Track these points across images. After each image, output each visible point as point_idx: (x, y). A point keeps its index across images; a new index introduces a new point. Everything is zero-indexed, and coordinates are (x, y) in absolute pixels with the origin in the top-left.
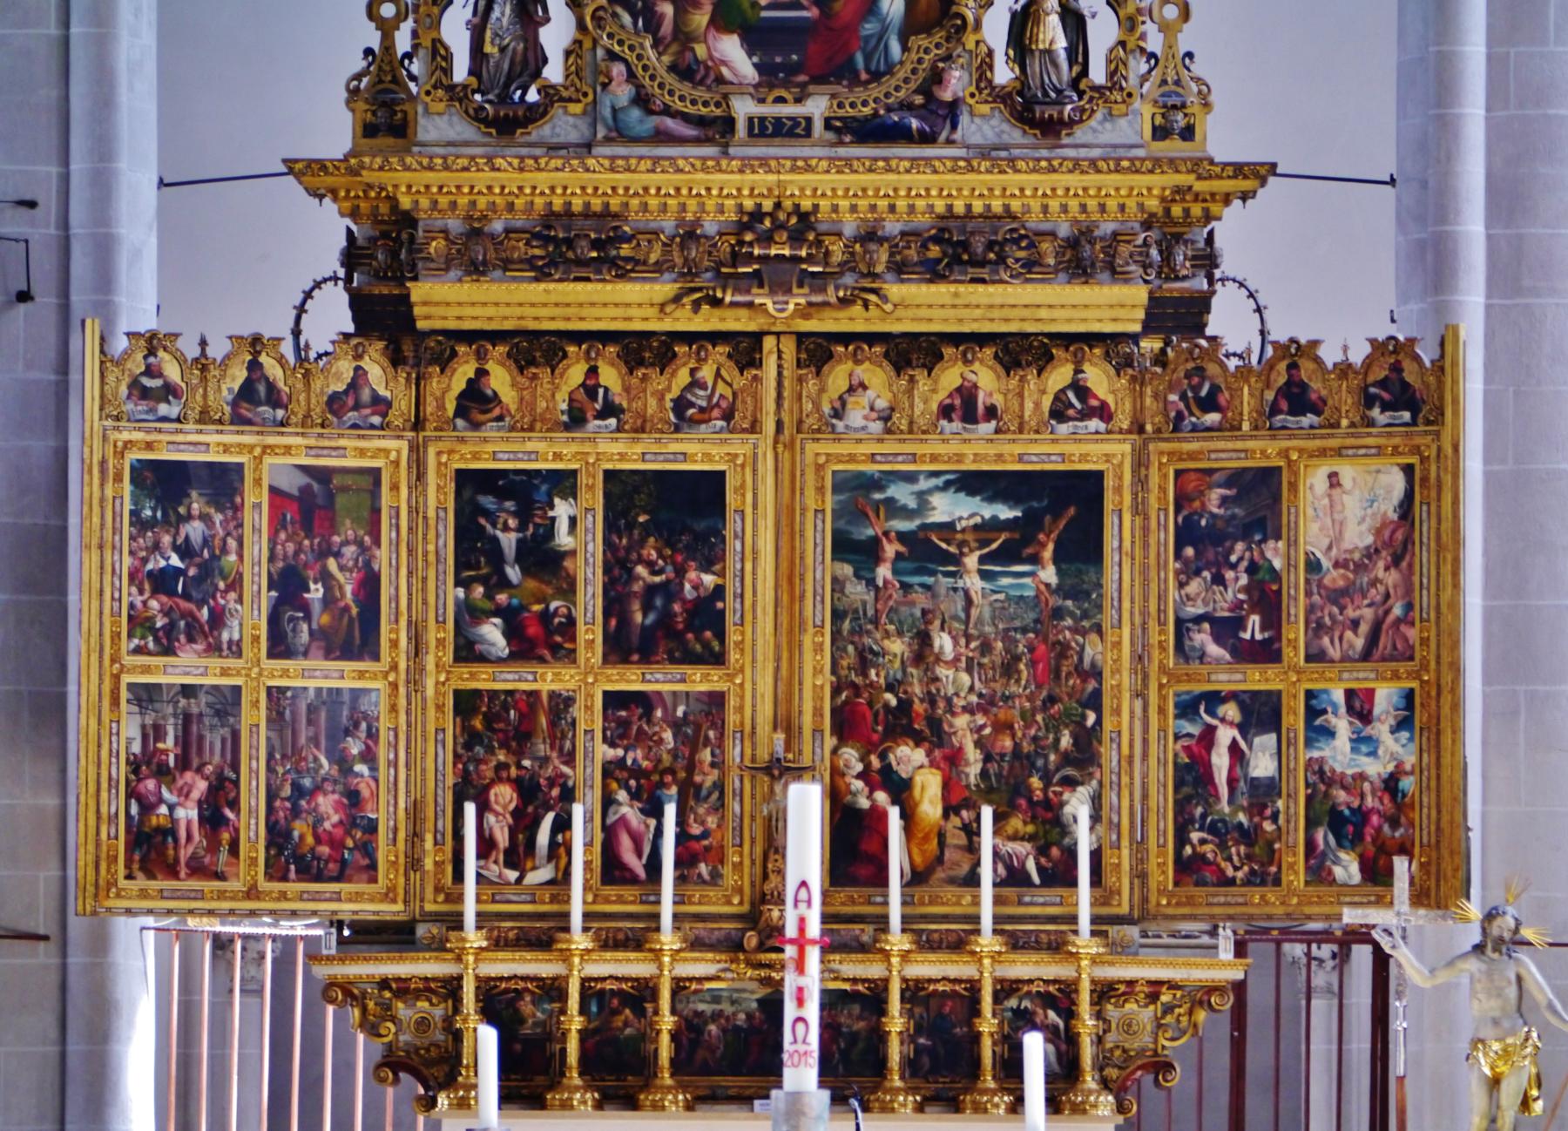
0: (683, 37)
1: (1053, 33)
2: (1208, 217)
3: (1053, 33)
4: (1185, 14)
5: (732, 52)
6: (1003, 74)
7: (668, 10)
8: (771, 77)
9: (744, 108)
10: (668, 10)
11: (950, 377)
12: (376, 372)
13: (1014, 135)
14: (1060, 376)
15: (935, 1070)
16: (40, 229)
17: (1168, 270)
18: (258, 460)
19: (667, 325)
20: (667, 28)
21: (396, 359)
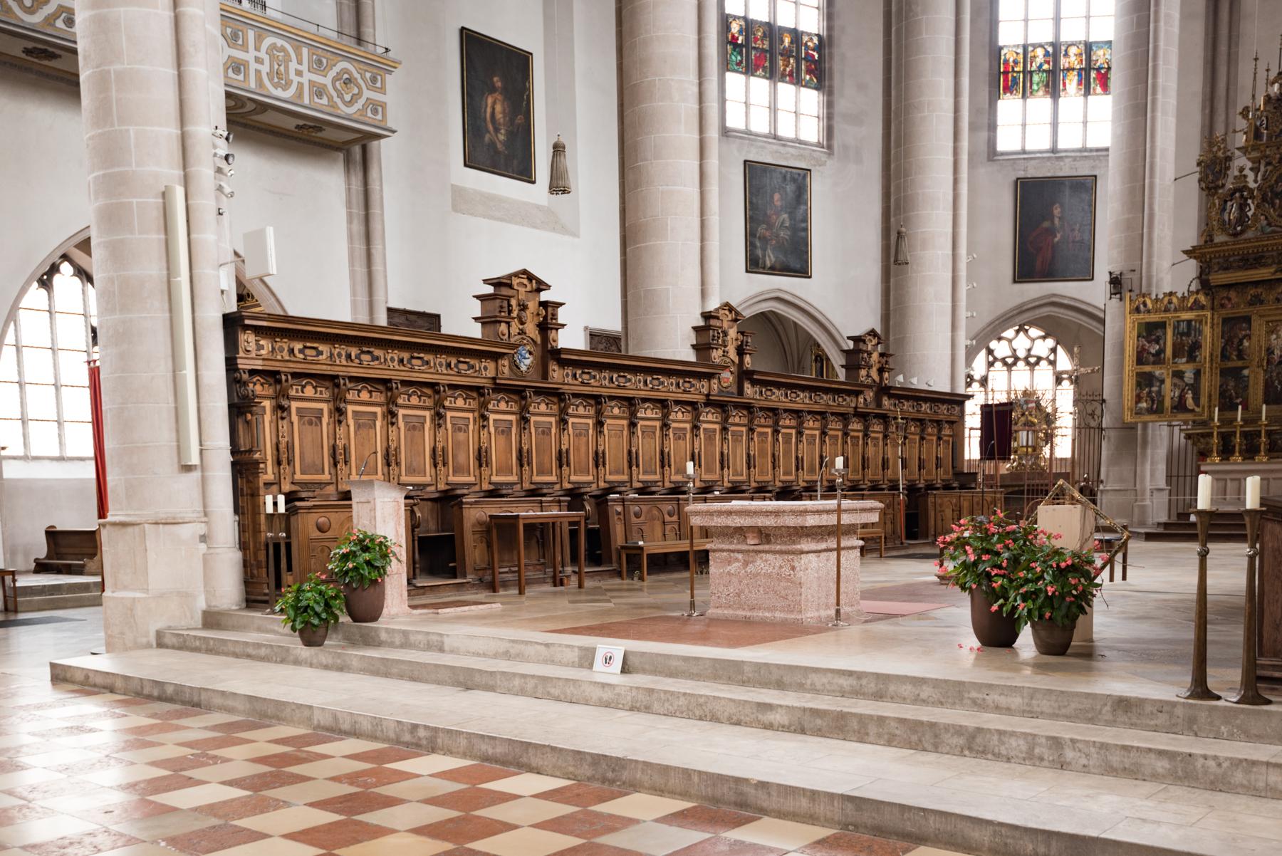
12: (1202, 298)
16: (1135, 276)
18: (1170, 320)
19: (1273, 277)
21: (1206, 295)
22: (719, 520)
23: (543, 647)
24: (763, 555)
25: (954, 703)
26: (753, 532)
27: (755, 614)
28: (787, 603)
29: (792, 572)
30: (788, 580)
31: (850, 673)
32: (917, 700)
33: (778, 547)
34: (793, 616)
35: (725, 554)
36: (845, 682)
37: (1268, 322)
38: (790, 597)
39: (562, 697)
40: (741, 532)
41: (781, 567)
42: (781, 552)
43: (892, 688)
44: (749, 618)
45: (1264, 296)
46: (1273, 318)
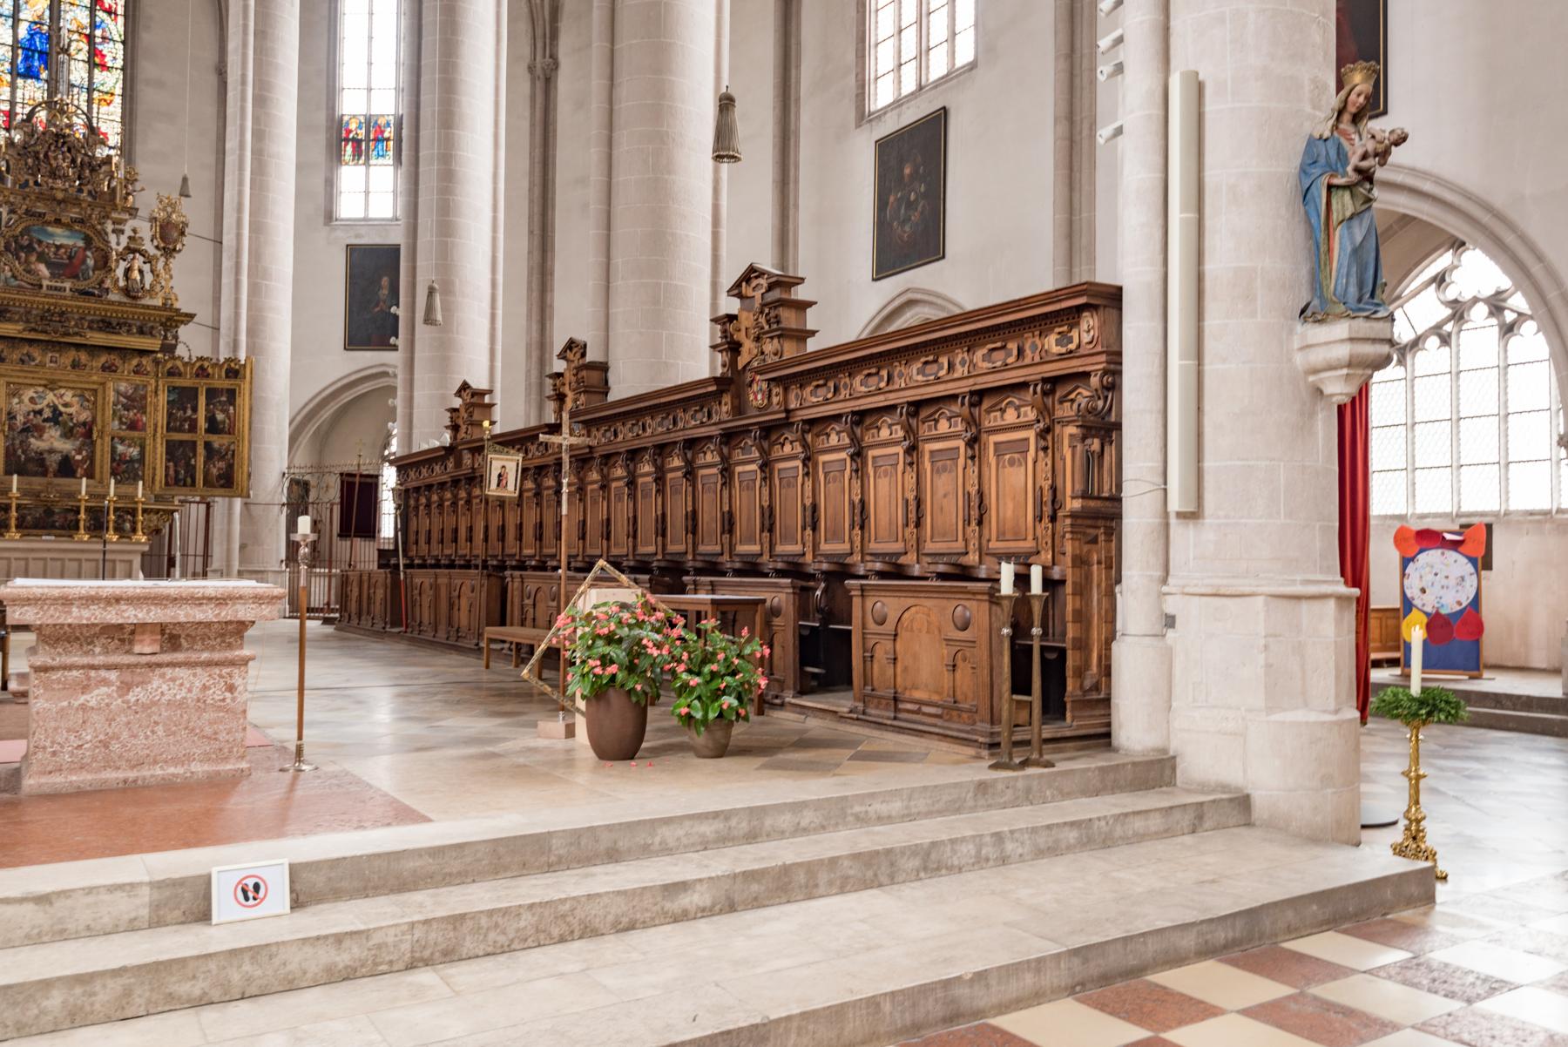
0: (27, 261)
1: (136, 275)
2: (177, 327)
3: (136, 275)
4: (171, 277)
5: (43, 269)
6: (122, 283)
7: (23, 255)
8: (53, 276)
9: (45, 283)
10: (23, 255)
11: (103, 359)
13: (125, 300)
14: (135, 362)
15: (95, 530)
17: (165, 337)
20: (23, 260)
22: (86, 613)
23: (30, 907)
24: (169, 672)
25: (837, 824)
26: (152, 633)
27: (146, 772)
28: (216, 745)
29: (228, 695)
30: (220, 709)
31: (716, 815)
32: (800, 830)
33: (205, 656)
34: (229, 767)
35: (75, 673)
36: (708, 829)
37: (8, 384)
38: (222, 736)
39: (215, 994)
40: (122, 635)
41: (205, 688)
42: (208, 664)
43: (768, 822)
44: (135, 781)
45: (5, 353)
46: (16, 380)
